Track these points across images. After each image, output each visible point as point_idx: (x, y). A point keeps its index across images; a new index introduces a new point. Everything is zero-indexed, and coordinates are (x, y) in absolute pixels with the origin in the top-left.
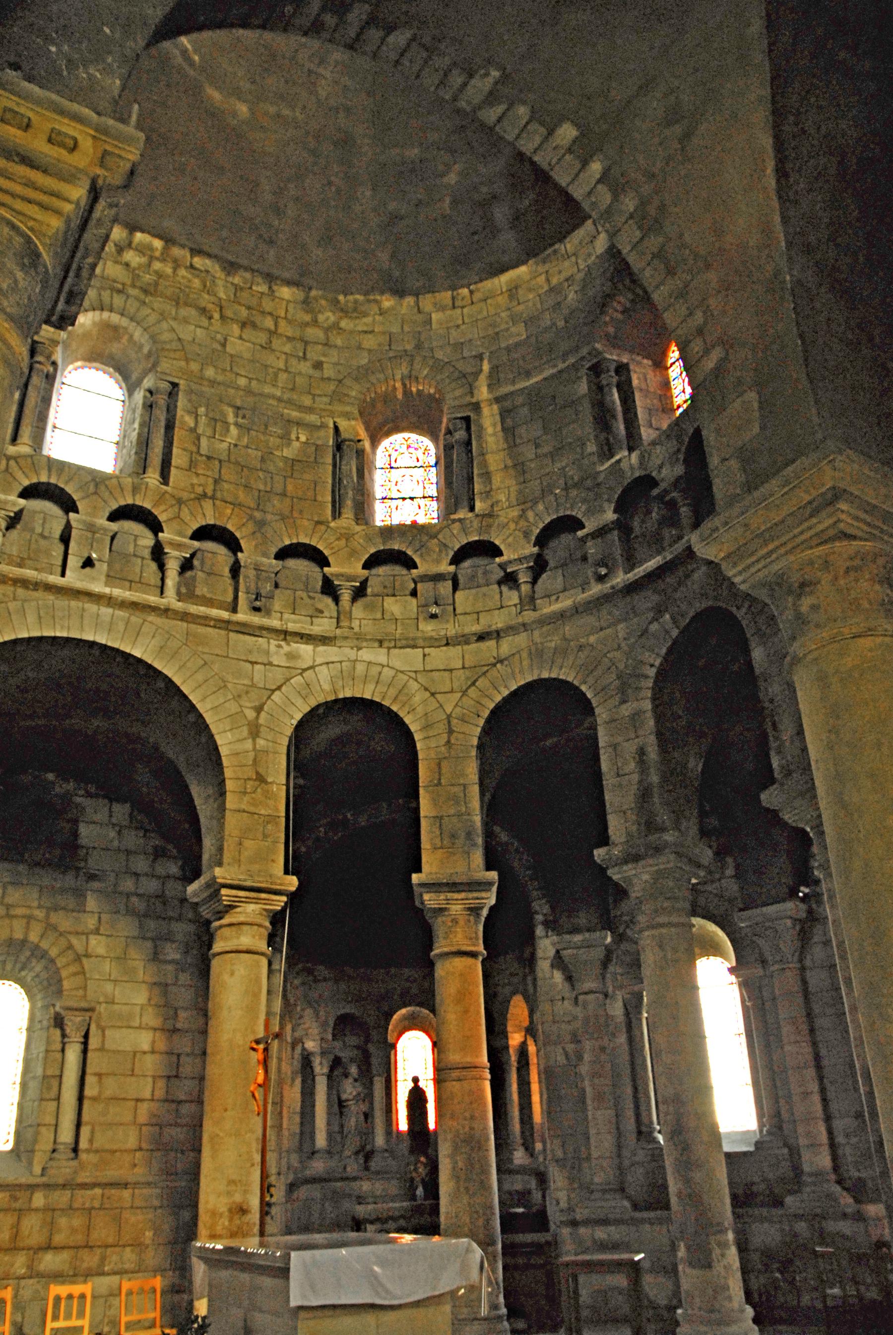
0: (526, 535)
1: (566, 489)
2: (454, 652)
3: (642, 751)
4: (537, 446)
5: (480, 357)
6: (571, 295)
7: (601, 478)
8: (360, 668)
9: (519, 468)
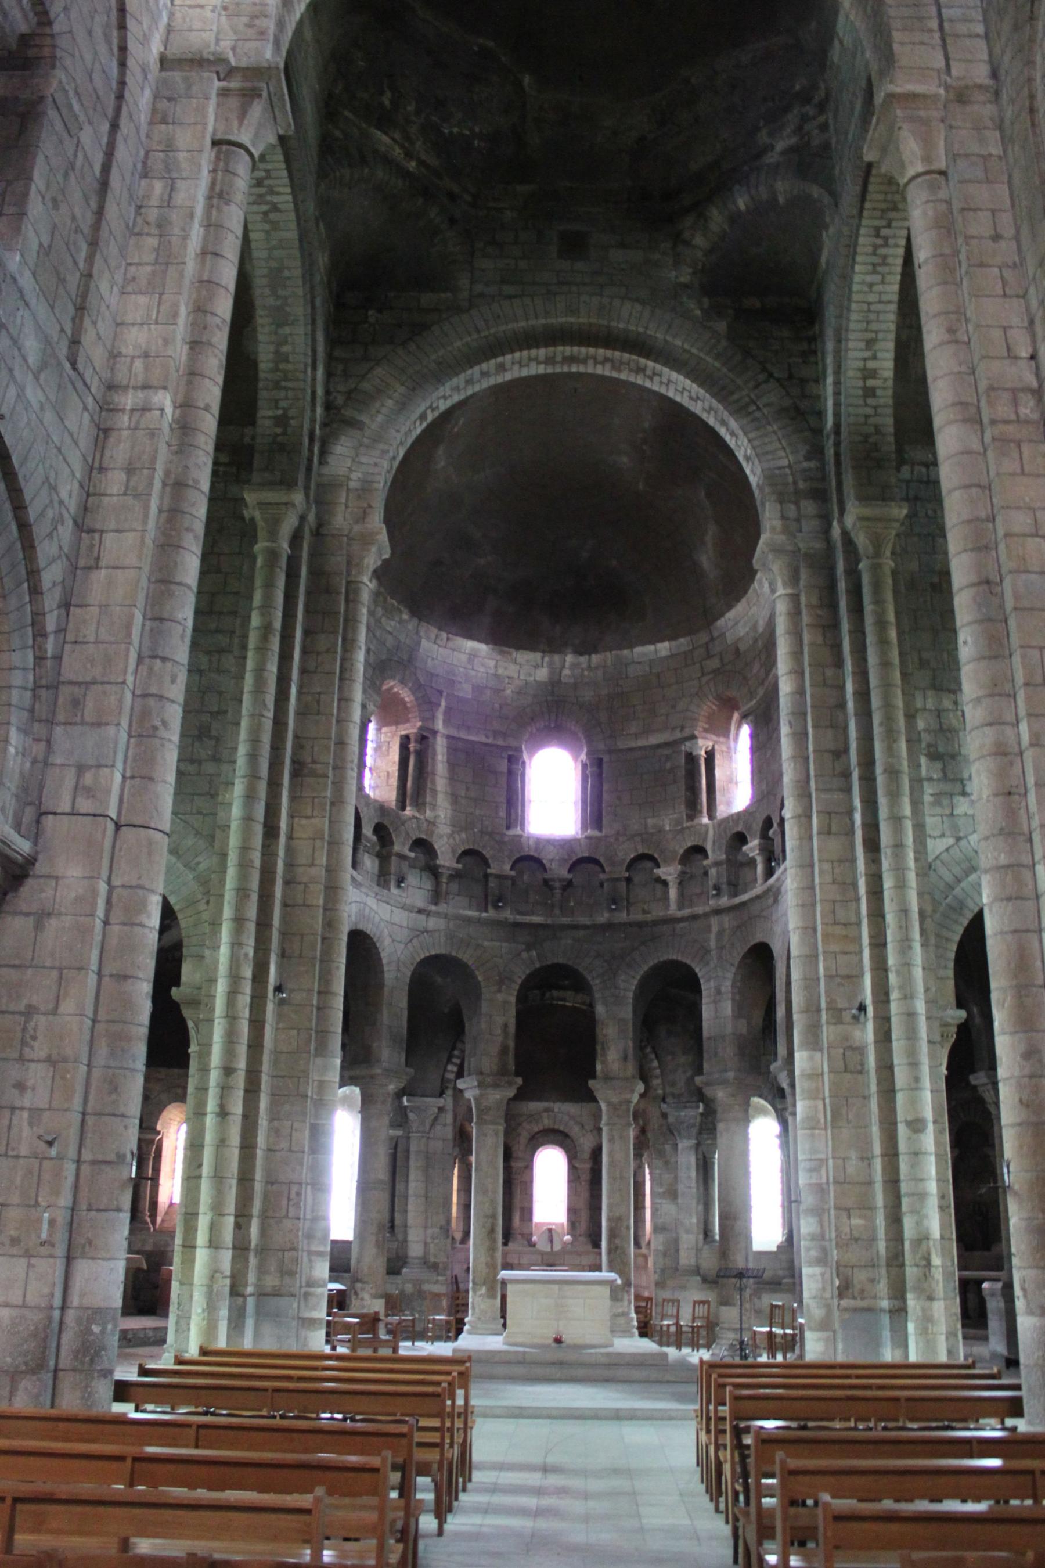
0: (453, 851)
1: (482, 832)
2: (405, 914)
3: (506, 1026)
4: (467, 789)
5: (440, 692)
6: (508, 692)
7: (506, 839)
8: (367, 910)
9: (454, 798)
